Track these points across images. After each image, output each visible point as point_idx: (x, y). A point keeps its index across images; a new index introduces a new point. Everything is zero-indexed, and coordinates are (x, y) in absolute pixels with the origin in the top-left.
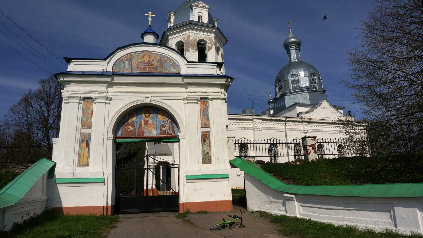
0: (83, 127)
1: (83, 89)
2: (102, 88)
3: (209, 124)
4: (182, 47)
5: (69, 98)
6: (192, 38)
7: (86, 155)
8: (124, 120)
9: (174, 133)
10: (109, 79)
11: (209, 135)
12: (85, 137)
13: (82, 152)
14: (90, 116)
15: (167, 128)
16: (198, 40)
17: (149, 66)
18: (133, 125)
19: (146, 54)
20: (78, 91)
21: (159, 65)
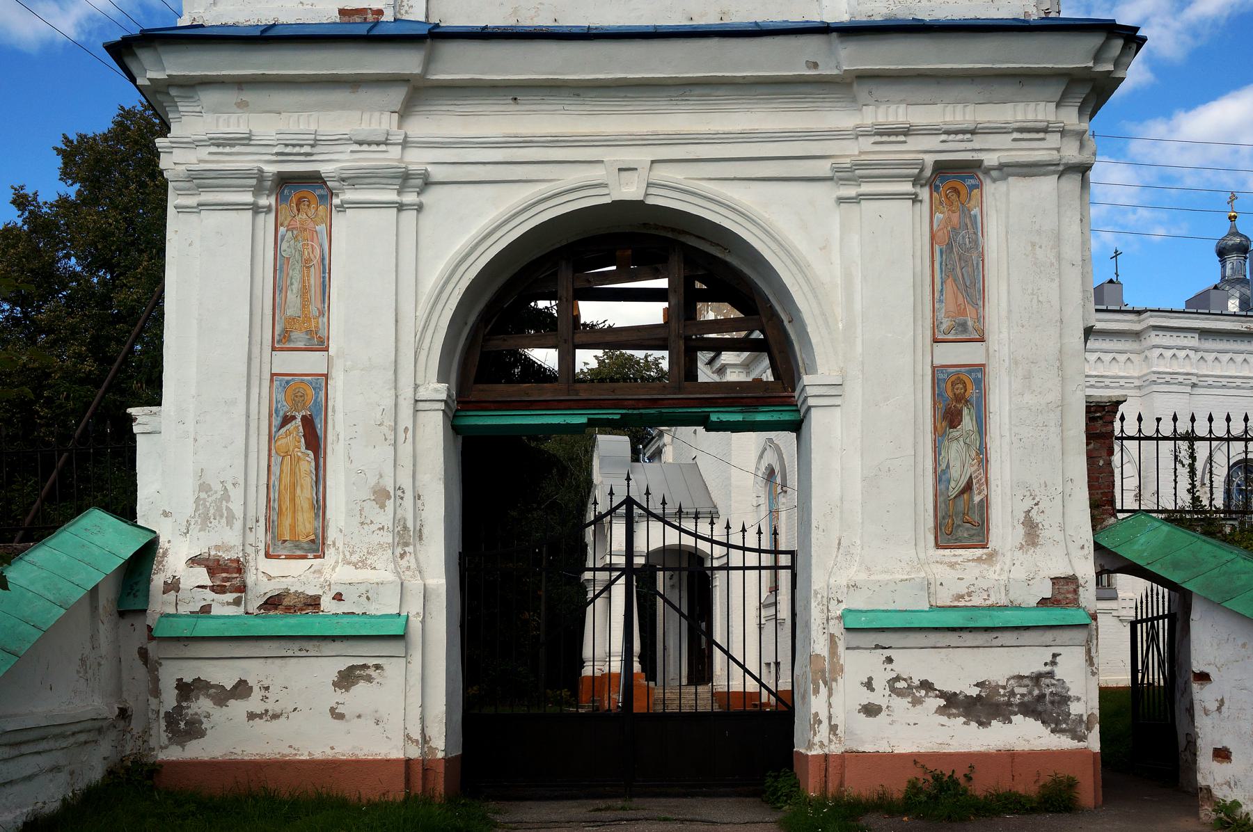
0: (282, 342)
1: (272, 129)
2: (372, 118)
3: (980, 319)
5: (198, 180)
7: (305, 494)
11: (980, 384)
12: (297, 399)
13: (287, 479)
14: (314, 281)
20: (247, 140)
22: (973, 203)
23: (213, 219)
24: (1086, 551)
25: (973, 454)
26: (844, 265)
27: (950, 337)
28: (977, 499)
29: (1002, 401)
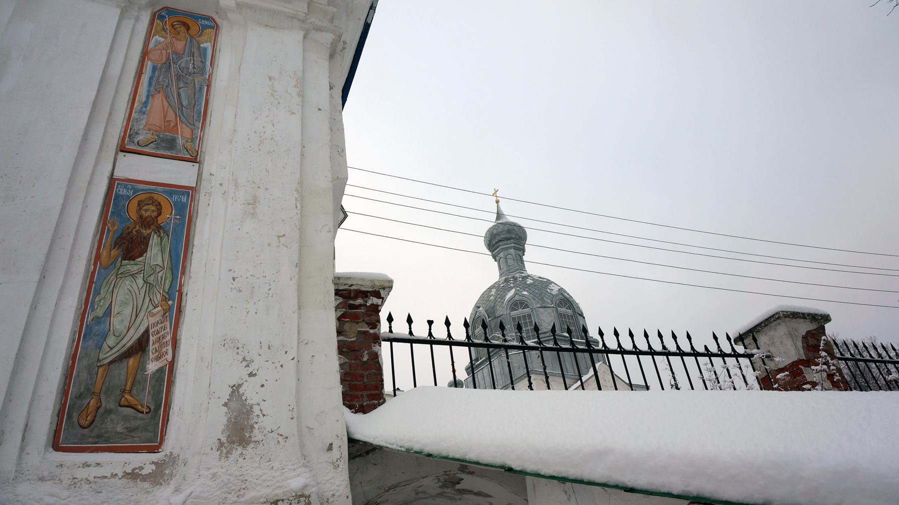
11: (181, 208)
22: (204, 38)
24: (336, 453)
25: (158, 298)
27: (147, 150)
28: (152, 367)
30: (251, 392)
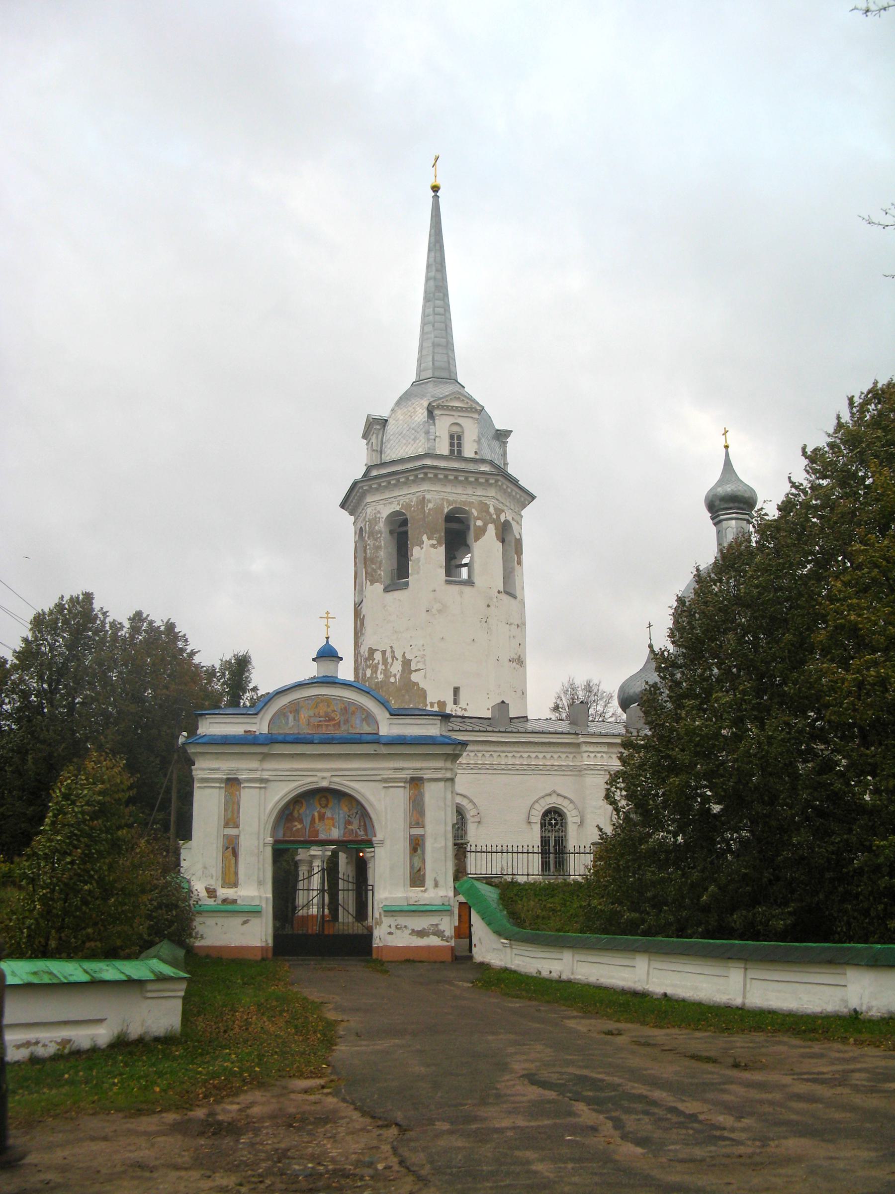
0: (226, 825)
2: (254, 764)
4: (403, 529)
6: (430, 506)
8: (287, 812)
9: (367, 835)
10: (264, 750)
15: (354, 826)
16: (446, 510)
17: (326, 721)
18: (301, 821)
19: (322, 701)
21: (342, 719)
23: (208, 791)
26: (386, 806)
29: (429, 845)
30: (438, 879)
